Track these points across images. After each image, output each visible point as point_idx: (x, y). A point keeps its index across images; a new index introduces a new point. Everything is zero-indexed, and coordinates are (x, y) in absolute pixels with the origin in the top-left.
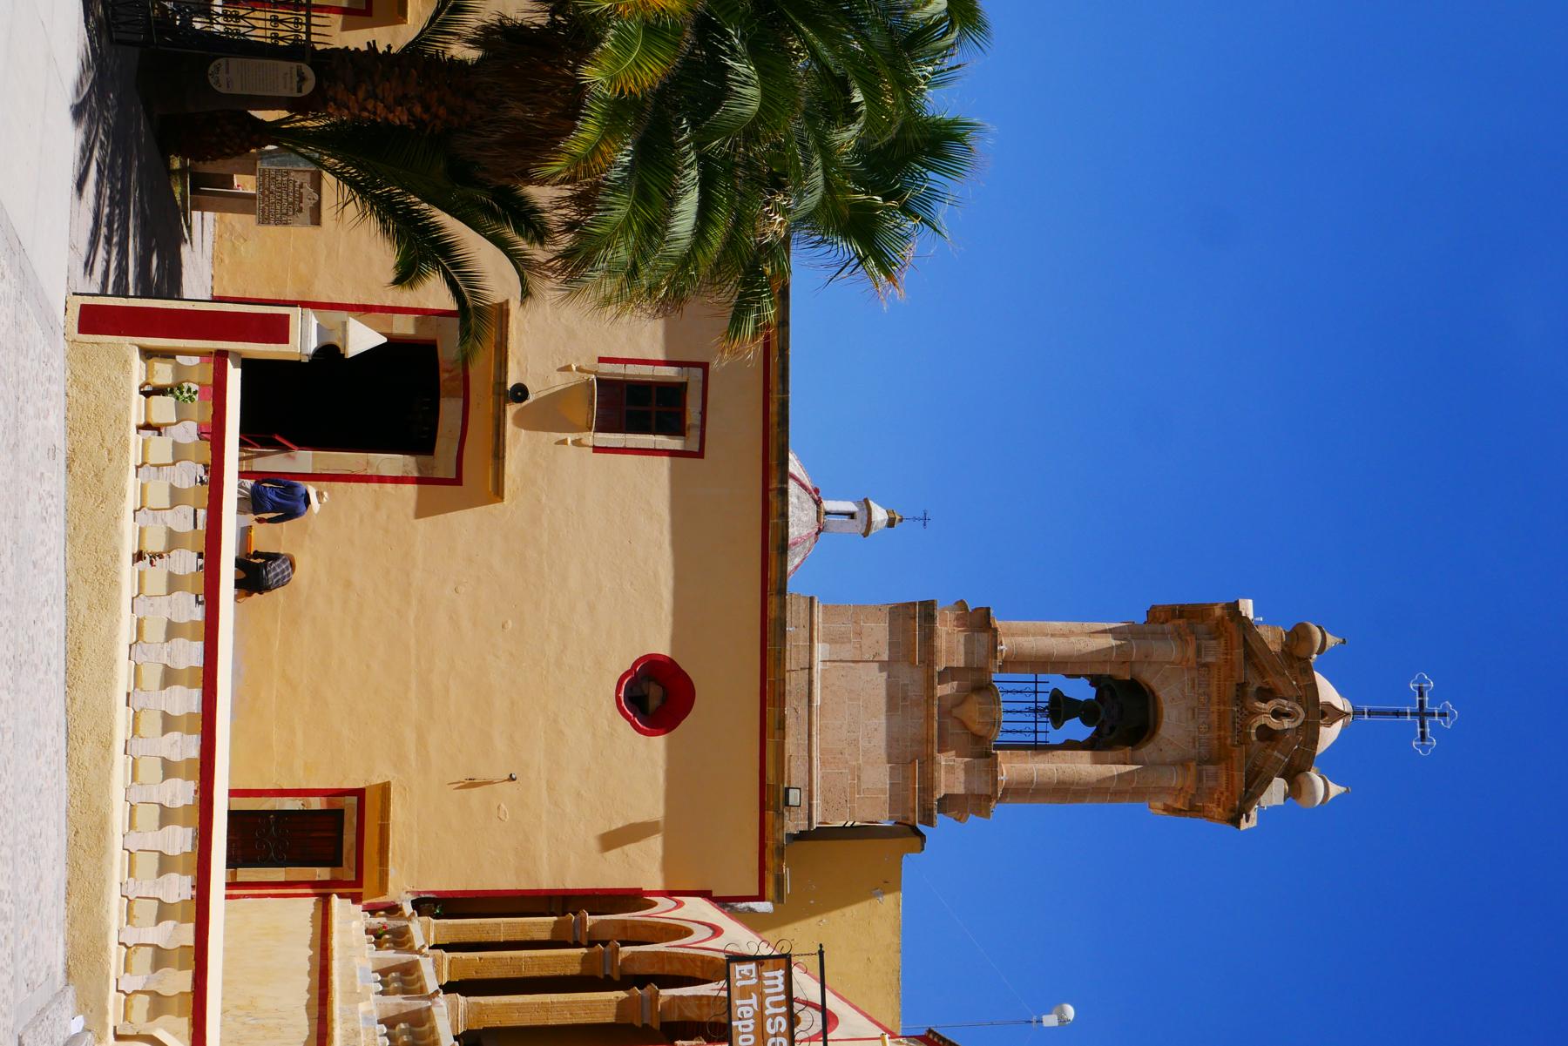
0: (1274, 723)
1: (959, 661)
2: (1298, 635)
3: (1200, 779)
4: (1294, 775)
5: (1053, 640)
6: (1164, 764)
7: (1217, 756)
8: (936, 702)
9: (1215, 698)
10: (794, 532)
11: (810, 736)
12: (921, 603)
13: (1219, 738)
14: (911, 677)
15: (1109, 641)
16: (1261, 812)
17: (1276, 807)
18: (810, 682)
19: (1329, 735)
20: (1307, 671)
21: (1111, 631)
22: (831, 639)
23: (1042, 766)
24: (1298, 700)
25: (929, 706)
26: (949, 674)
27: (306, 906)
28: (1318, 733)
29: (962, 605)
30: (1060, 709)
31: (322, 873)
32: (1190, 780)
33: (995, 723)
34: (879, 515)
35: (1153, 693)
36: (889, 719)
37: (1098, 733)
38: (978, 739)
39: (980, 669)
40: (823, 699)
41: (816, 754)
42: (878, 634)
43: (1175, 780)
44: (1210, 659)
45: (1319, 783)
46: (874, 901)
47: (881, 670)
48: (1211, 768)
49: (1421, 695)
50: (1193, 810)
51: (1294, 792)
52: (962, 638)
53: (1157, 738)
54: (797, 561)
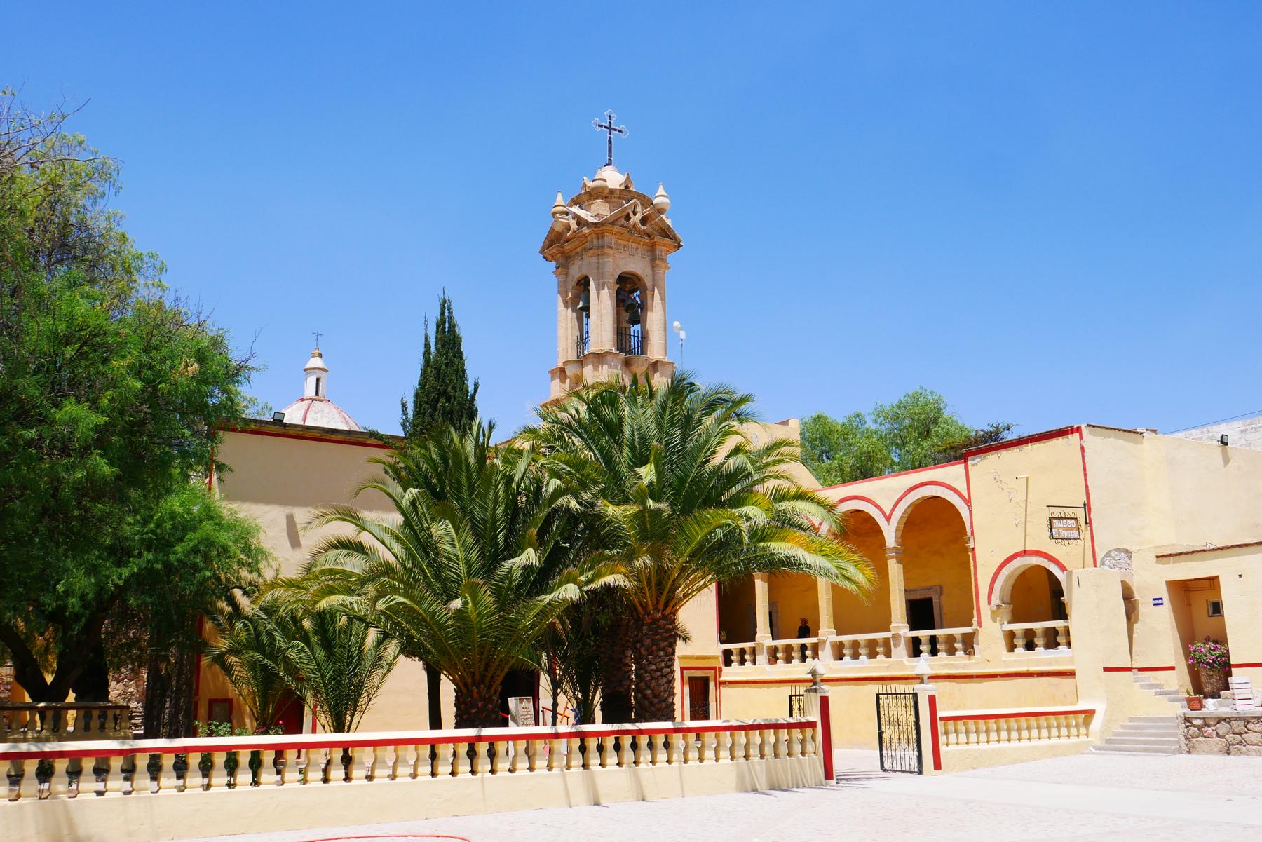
0: (639, 216)
7: (652, 248)
27: (724, 690)
31: (712, 685)
34: (315, 362)
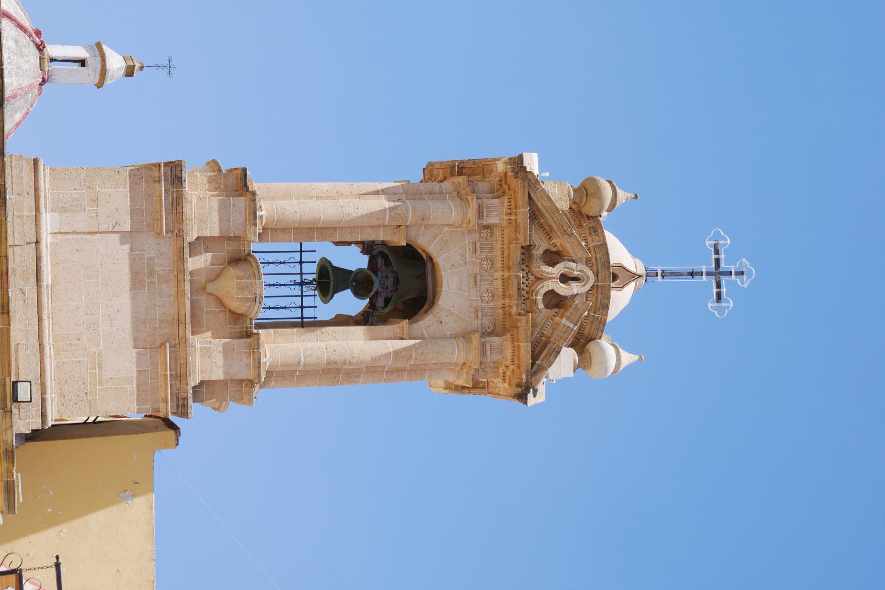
0: (562, 289)
1: (213, 230)
2: (586, 191)
3: (484, 353)
4: (582, 343)
5: (319, 204)
6: (445, 337)
7: (502, 327)
8: (188, 277)
9: (498, 264)
10: (11, 83)
11: (40, 320)
12: (167, 164)
13: (503, 307)
14: (159, 250)
15: (382, 203)
16: (549, 386)
17: (566, 379)
18: (38, 259)
19: (620, 299)
20: (596, 229)
21: (383, 191)
22: (62, 208)
23: (309, 345)
24: (588, 262)
25: (179, 282)
26: (203, 243)
28: (609, 298)
29: (214, 165)
30: (328, 280)
32: (473, 356)
33: (255, 299)
34: (116, 63)
35: (431, 259)
36: (133, 298)
37: (372, 305)
38: (237, 317)
39: (237, 238)
40: (54, 278)
41: (48, 341)
42: (117, 203)
43: (455, 353)
44: (493, 220)
45: (610, 352)
46: (122, 506)
47: (122, 243)
48: (495, 340)
49: (717, 252)
50: (477, 386)
51: (584, 361)
52: (215, 203)
53: (436, 309)
54: (18, 117)
